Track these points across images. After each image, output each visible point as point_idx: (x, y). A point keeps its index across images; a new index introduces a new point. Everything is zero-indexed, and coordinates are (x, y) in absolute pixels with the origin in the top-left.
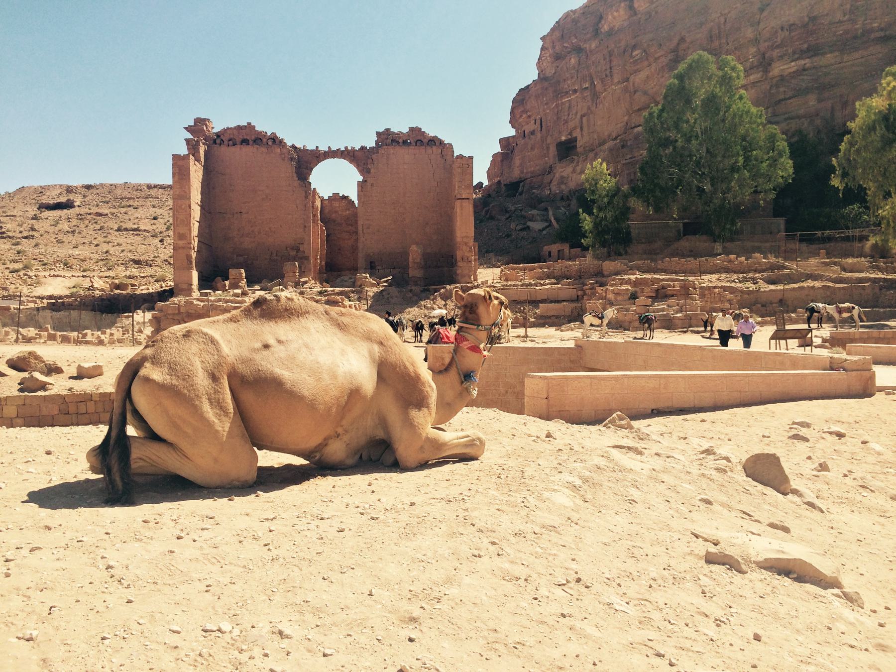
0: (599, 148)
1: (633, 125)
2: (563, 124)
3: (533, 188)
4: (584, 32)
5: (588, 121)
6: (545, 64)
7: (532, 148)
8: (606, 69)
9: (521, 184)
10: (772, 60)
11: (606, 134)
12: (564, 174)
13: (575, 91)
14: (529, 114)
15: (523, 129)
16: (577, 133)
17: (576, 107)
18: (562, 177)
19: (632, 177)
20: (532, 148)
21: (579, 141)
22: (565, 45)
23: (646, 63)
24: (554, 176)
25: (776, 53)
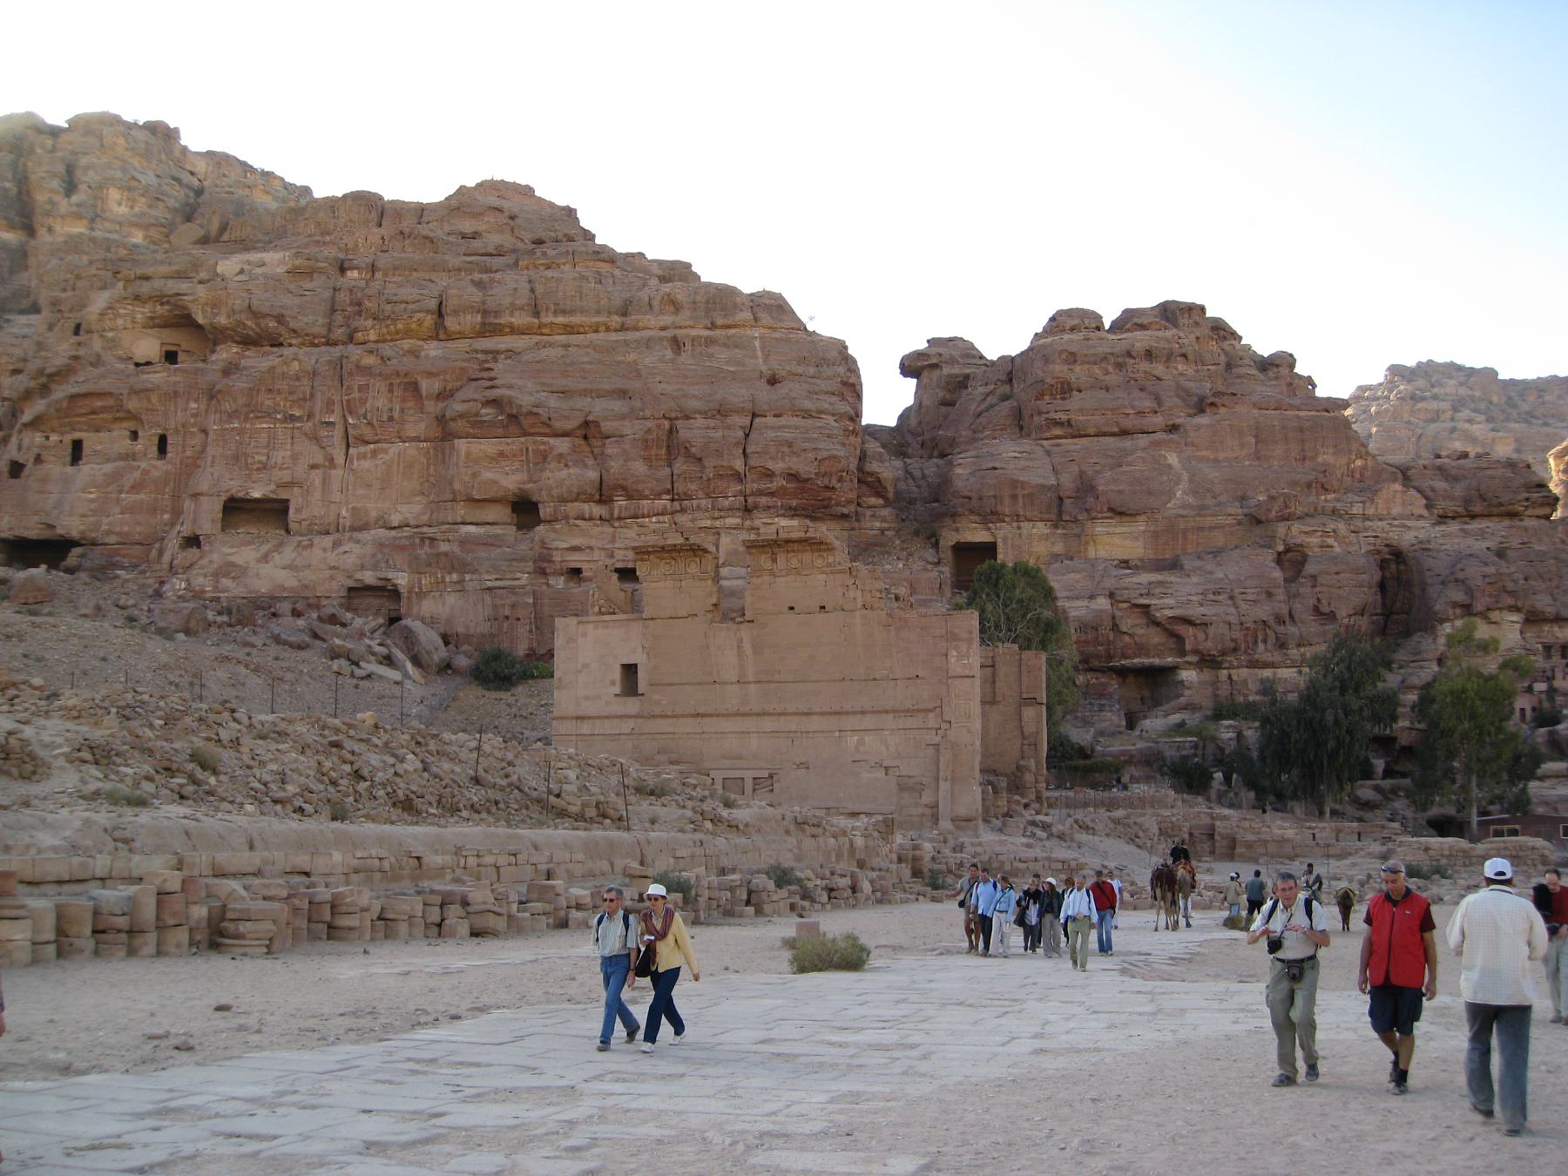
0: (347, 535)
1: (459, 520)
2: (258, 469)
3: (115, 566)
4: (306, 320)
5: (326, 482)
6: (120, 322)
7: (133, 487)
8: (391, 410)
9: (76, 551)
10: (756, 507)
11: (374, 514)
12: (239, 559)
13: (292, 418)
14: (118, 415)
15: (77, 435)
16: (296, 499)
17: (289, 447)
18: (232, 564)
19: (507, 612)
20: (136, 487)
21: (298, 511)
22: (249, 323)
23: (500, 431)
24: (201, 558)
25: (764, 500)
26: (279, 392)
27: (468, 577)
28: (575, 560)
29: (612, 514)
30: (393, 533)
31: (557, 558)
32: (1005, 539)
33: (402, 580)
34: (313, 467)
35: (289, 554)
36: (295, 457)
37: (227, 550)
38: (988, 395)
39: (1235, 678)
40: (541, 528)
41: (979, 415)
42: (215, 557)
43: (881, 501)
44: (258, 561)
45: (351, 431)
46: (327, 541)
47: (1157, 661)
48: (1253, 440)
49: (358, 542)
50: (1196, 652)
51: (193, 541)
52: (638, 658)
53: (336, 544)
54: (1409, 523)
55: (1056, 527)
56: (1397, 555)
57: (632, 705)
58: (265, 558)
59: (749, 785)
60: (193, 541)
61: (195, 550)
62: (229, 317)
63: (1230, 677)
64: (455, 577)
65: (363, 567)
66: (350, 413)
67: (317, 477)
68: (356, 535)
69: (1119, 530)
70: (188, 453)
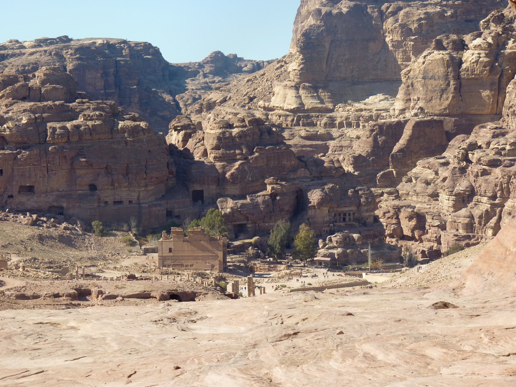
13: (35, 165)
19: (93, 214)
21: (37, 188)
25: (150, 183)
26: (32, 159)
27: (82, 204)
28: (106, 199)
29: (114, 188)
30: (60, 193)
31: (102, 199)
32: (206, 189)
33: (65, 205)
34: (40, 177)
35: (35, 198)
36: (36, 175)
37: (20, 198)
38: (197, 143)
39: (260, 225)
40: (97, 191)
41: (195, 149)
42: (17, 200)
43: (172, 176)
44: (27, 200)
45: (49, 168)
46: (44, 195)
47: (242, 223)
48: (266, 160)
49: (51, 195)
50: (251, 220)
51: (11, 196)
52: (172, 247)
53: (46, 196)
54: (304, 180)
55: (218, 186)
56: (301, 190)
57: (171, 254)
58: (29, 200)
59: (189, 266)
60: (11, 196)
61: (11, 198)
62: (15, 138)
63: (259, 225)
64: (78, 204)
65: (53, 201)
66: (49, 163)
67: (41, 179)
68: (51, 193)
69: (233, 187)
70: (8, 174)
